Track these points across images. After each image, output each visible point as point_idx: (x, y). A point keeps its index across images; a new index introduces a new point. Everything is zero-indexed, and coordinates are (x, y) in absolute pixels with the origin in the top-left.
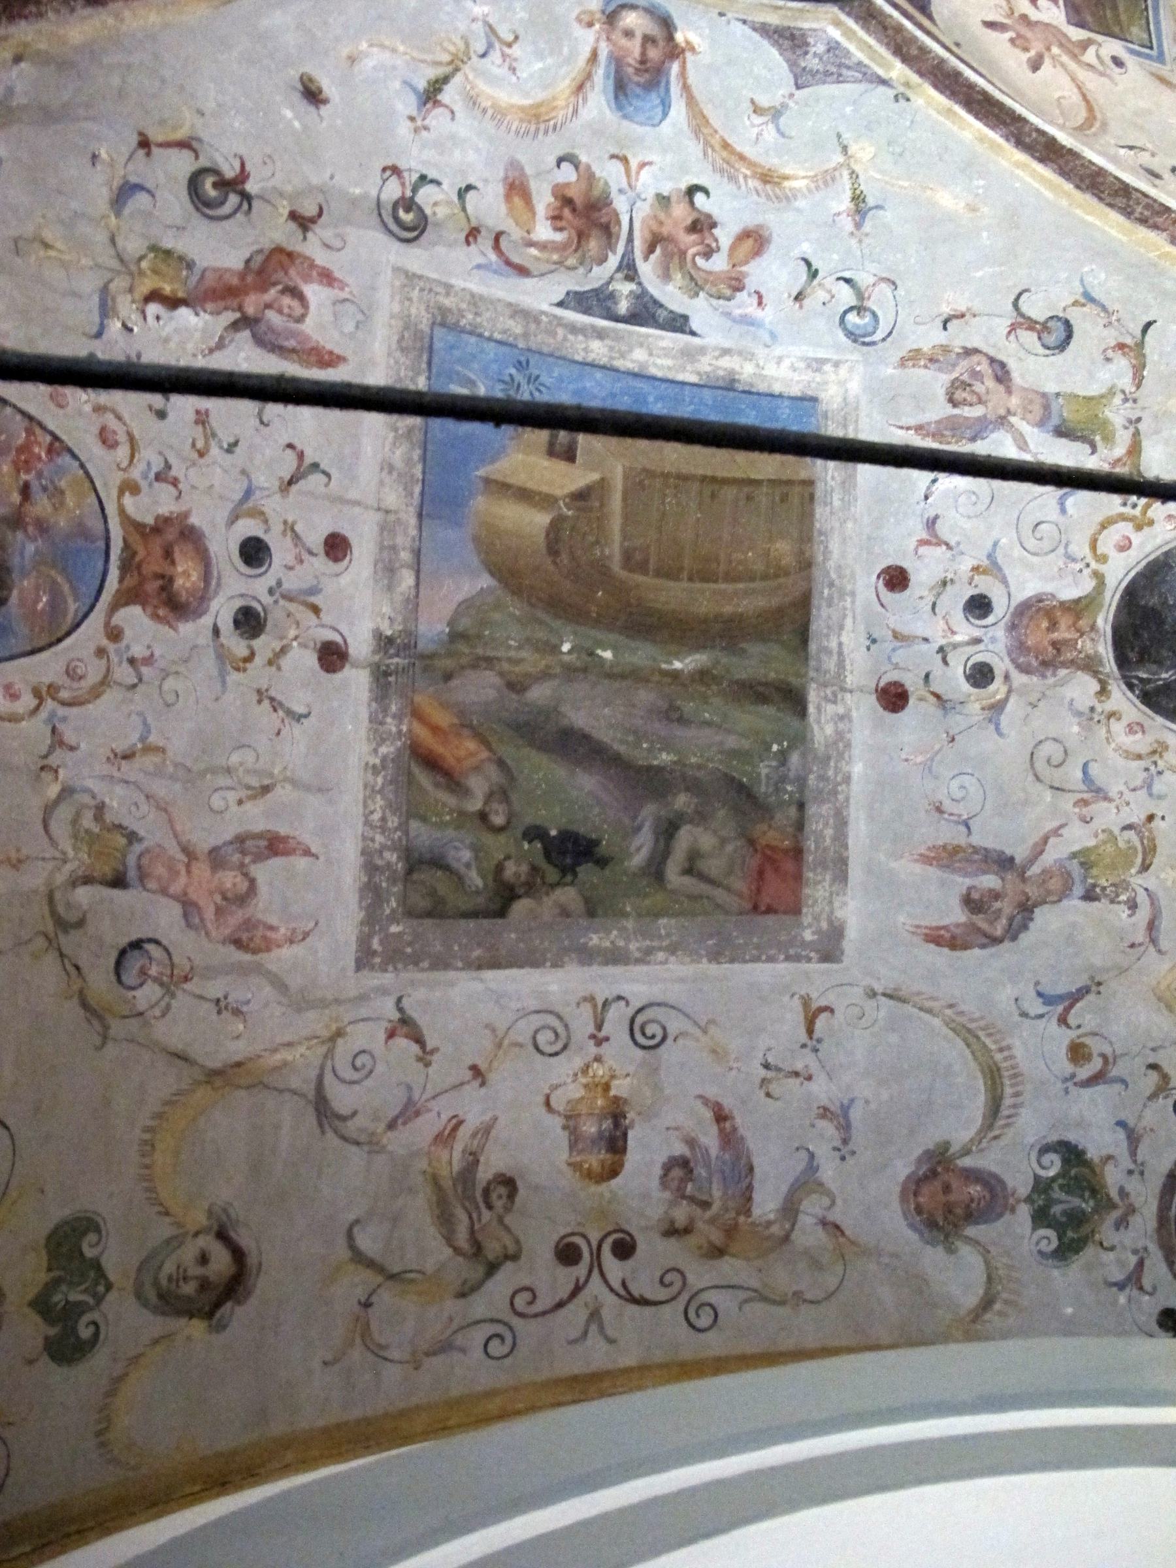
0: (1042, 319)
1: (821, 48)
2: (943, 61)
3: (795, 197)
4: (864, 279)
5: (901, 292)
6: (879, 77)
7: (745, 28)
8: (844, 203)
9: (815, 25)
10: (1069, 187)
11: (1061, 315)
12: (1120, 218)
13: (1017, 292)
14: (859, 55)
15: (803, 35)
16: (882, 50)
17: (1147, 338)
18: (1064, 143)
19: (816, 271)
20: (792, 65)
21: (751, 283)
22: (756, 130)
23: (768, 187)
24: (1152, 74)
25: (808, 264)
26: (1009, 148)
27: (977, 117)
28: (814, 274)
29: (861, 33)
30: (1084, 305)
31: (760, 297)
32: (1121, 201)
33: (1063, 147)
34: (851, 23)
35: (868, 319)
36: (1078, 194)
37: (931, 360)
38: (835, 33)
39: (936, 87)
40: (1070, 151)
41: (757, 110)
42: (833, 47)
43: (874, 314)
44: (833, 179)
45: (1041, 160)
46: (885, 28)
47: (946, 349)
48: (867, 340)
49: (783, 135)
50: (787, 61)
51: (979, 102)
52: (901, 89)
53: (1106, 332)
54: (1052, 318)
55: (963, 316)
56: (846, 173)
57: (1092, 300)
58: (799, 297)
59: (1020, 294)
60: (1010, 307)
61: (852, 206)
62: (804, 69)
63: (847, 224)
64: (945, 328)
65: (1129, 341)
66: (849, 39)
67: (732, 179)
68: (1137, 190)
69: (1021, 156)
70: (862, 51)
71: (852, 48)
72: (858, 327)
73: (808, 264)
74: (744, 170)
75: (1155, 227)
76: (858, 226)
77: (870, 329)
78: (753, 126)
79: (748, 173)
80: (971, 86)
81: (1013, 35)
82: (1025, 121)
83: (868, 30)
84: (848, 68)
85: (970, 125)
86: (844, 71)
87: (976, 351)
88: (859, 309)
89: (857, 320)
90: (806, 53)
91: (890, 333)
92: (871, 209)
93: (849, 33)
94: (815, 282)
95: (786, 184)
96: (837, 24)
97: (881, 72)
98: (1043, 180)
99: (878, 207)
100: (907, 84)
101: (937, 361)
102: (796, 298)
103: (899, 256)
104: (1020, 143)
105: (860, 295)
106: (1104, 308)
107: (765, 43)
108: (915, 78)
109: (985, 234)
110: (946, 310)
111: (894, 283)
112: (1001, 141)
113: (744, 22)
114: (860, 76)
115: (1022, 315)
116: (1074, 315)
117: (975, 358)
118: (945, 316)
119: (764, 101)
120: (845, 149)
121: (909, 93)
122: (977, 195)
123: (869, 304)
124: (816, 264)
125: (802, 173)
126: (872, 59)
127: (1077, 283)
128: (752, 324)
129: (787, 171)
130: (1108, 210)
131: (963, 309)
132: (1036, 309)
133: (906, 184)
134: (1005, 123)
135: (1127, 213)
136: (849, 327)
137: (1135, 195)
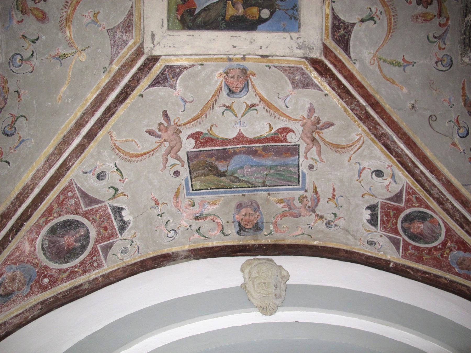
0: (15, 126)
1: (125, 38)
2: (119, 84)
3: (62, 32)
4: (34, 61)
5: (29, 75)
6: (113, 61)
7: (130, 7)
8: (61, 52)
9: (134, 34)
10: (65, 133)
11: (16, 132)
12: (50, 152)
13: (27, 117)
14: (122, 53)
15: (130, 31)
16: (124, 61)
17: (3, 162)
18: (82, 130)
19: (35, 43)
20: (117, 27)
21: (25, 17)
22: (87, 14)
23: (65, 21)
24: (179, 189)
25: (37, 39)
26: (82, 110)
27: (96, 98)
28: (34, 42)
29: (130, 53)
30: (19, 140)
31: (22, 21)
32: (56, 152)
33: (81, 130)
34: (135, 48)
35: (19, 63)
36: (62, 136)
37: (3, 87)
38: (130, 43)
39: (108, 82)
40: (79, 133)
41: (95, 15)
42: (125, 42)
43: (20, 65)
44: (71, 46)
45: (76, 122)
46: (132, 61)
47: (7, 92)
48: (11, 63)
49: (87, 25)
50: (119, 25)
51: (101, 98)
52: (108, 69)
53: (8, 148)
54: (16, 129)
55: (19, 98)
56: (74, 51)
57: (21, 143)
58: (24, 37)
59: (25, 117)
60: (21, 114)
61: (61, 54)
62: (116, 32)
63: (54, 53)
64: (15, 92)
65: (3, 156)
66: (129, 48)
67: (65, 7)
68: (60, 157)
69: (79, 115)
70: (123, 53)
71: (125, 50)
72: (15, 60)
73: (37, 39)
74: (69, 11)
75: (45, 164)
76: (53, 57)
77: (15, 65)
78: (89, 13)
79: (69, 13)
80: (108, 95)
81: (166, 125)
82: (92, 116)
83: (133, 54)
84: (117, 49)
85: (92, 96)
86: (116, 47)
87: (6, 103)
88: (22, 60)
89: (18, 60)
90: (122, 32)
91: (14, 72)
92: (61, 62)
93: (131, 47)
94: (31, 43)
95: (67, 28)
96: (135, 43)
97: (115, 61)
98: (69, 124)
99: (61, 63)
100: (110, 71)
101: (3, 89)
102: (23, 36)
103: (42, 73)
104: (84, 114)
105: (27, 60)
106: (17, 147)
107: (124, 16)
108: (112, 74)
109: (50, 104)
110: (22, 92)
111: (32, 72)
112: (85, 108)
113: (132, 7)
114: (114, 54)
115: (17, 119)
116: (16, 137)
117: (3, 103)
118: (19, 91)
119: (100, 17)
120: (84, 50)
121: (107, 72)
122: (65, 100)
123: (24, 63)
124: (37, 42)
125: (72, 34)
126: (120, 57)
127: (28, 138)
128: (10, 19)
129: (72, 29)
130: (55, 147)
131: (22, 97)
132: (20, 123)
133: (70, 74)
134: (92, 108)
135: (52, 154)
136: (15, 57)
137: (58, 157)
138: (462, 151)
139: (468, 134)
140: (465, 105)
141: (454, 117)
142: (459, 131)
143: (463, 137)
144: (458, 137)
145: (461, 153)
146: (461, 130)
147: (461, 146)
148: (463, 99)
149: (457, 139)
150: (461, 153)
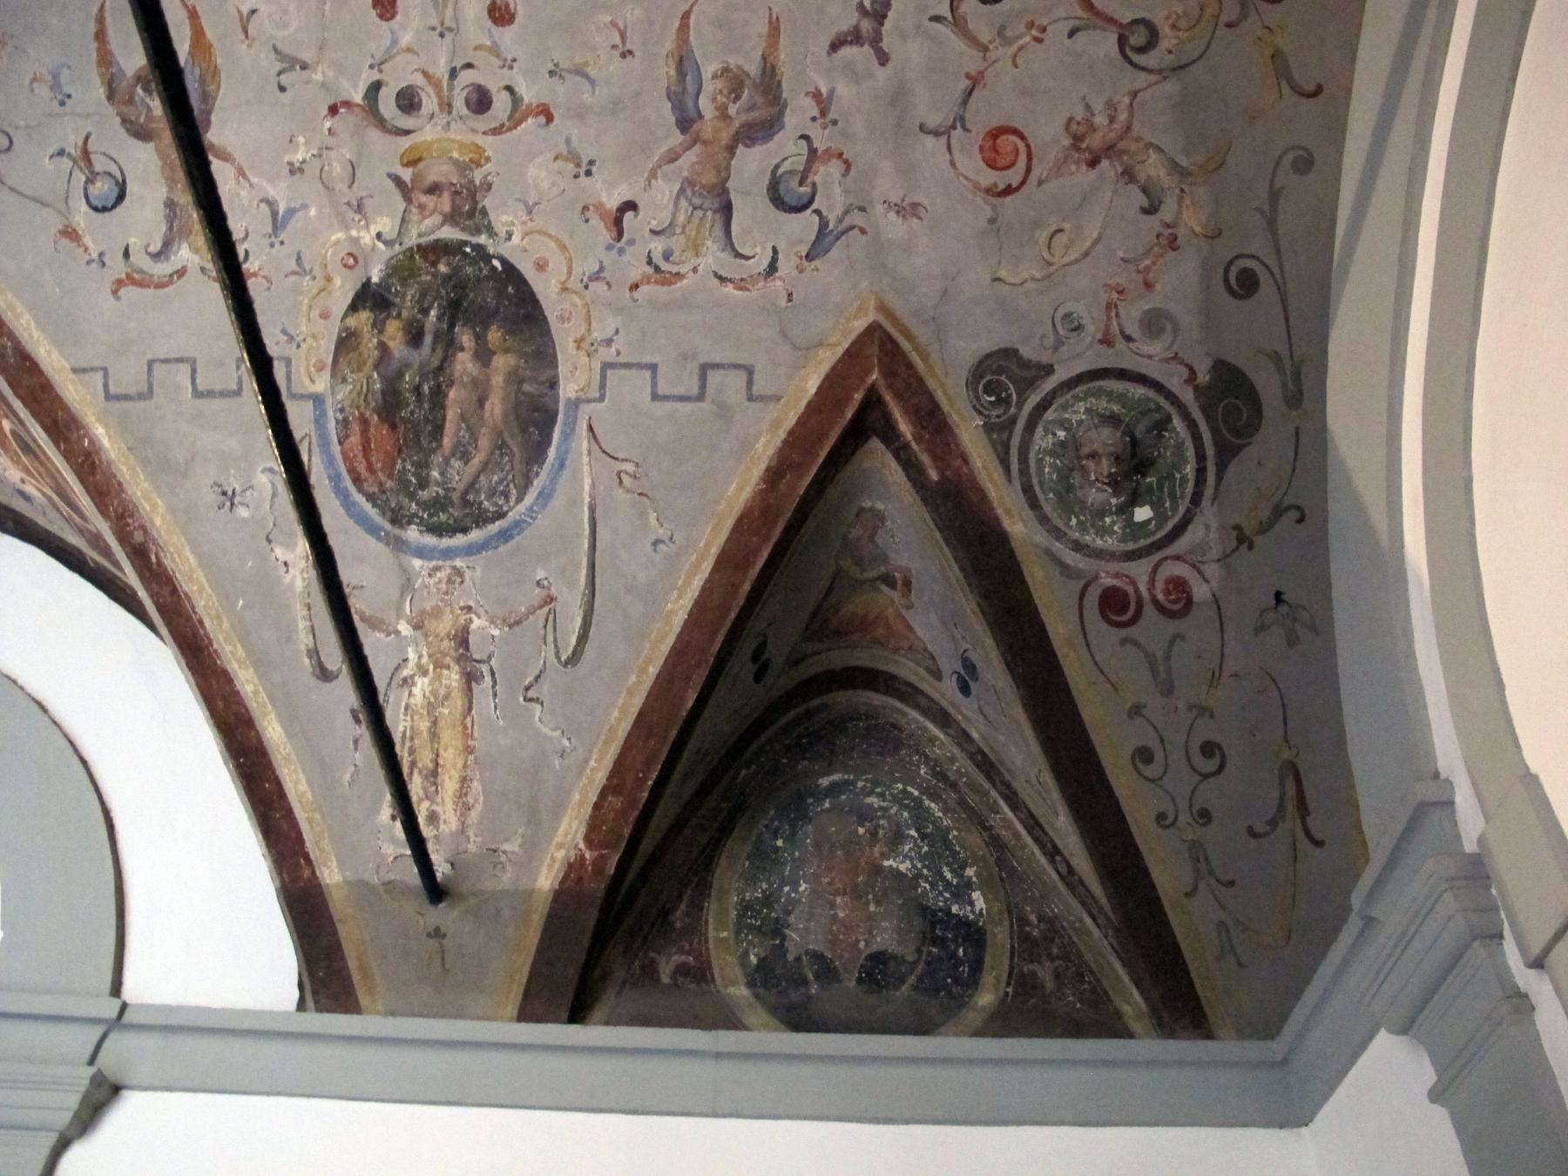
138: (95, 256)
139: (121, 197)
140: (111, 96)
141: (72, 143)
142: (93, 190)
143: (104, 209)
144: (84, 207)
145: (88, 263)
146: (98, 184)
147: (95, 242)
148: (102, 76)
149: (81, 215)
150: (88, 263)
